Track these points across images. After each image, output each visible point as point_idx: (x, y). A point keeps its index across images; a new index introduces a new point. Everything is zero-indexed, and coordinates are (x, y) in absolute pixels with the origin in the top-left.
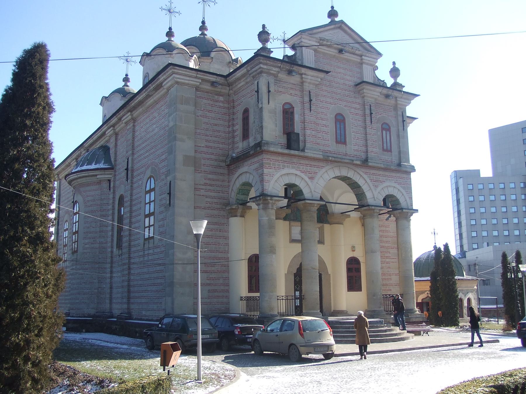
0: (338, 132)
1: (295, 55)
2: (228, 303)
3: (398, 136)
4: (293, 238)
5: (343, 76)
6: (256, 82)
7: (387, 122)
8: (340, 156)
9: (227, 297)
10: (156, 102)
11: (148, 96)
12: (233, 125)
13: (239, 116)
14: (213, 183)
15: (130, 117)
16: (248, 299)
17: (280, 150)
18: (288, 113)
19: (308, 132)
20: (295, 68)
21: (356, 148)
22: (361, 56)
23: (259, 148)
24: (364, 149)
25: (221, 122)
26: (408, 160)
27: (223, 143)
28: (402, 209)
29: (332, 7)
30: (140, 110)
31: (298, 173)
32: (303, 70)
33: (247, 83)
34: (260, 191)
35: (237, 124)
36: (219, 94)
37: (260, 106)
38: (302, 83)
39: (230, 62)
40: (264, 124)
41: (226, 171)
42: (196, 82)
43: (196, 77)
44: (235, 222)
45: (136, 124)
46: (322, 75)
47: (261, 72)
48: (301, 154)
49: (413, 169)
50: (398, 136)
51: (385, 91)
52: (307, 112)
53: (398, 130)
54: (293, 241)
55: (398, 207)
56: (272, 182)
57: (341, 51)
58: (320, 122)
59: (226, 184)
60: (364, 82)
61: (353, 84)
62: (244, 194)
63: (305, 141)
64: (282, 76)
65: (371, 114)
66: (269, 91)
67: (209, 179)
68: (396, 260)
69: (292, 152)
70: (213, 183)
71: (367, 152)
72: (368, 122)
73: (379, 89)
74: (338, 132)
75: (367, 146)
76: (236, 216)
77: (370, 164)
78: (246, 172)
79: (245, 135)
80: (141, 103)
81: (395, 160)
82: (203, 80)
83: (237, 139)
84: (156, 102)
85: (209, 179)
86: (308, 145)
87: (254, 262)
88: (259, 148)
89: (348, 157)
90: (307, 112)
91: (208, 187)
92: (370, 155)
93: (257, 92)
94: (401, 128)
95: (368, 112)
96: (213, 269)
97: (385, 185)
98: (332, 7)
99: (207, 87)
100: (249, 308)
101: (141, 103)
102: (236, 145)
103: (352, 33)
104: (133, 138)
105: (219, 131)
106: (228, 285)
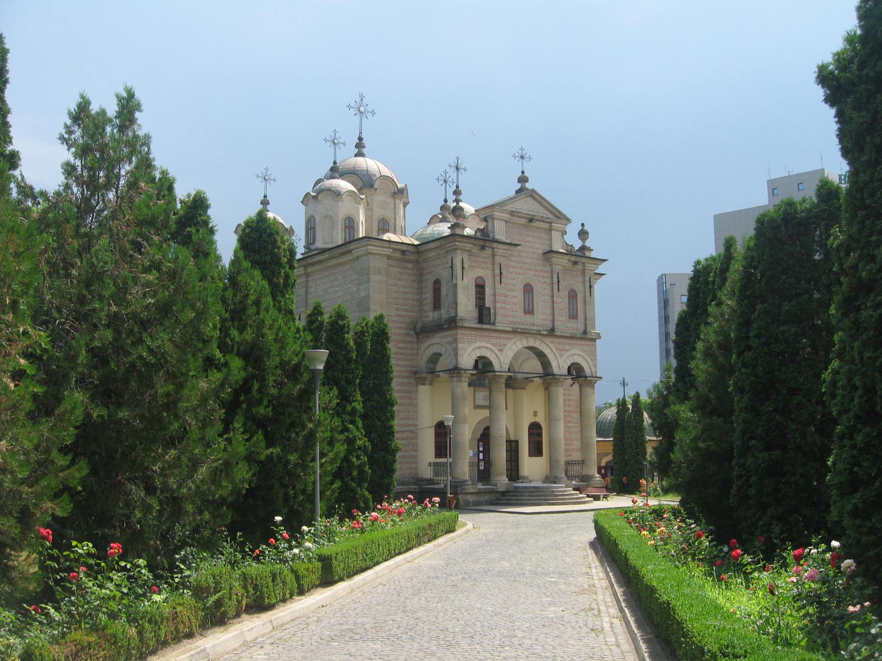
0: (527, 302)
1: (486, 227)
2: (416, 469)
3: (585, 302)
4: (477, 404)
5: (533, 244)
6: (450, 257)
7: (575, 288)
8: (527, 327)
9: (416, 463)
10: (341, 265)
11: (332, 258)
12: (421, 293)
13: (430, 286)
14: (403, 351)
15: (303, 272)
16: (435, 465)
17: (473, 326)
18: (480, 288)
19: (498, 305)
20: (488, 244)
21: (543, 317)
22: (550, 223)
23: (452, 323)
24: (550, 318)
25: (410, 290)
26: (594, 328)
27: (412, 311)
28: (586, 377)
29: (523, 172)
30: (318, 267)
31: (489, 346)
32: (495, 245)
33: (439, 254)
34: (454, 363)
35: (427, 292)
36: (408, 261)
37: (455, 282)
38: (493, 256)
39: (395, 193)
40: (459, 300)
41: (415, 340)
42: (388, 252)
43: (388, 248)
44: (424, 391)
45: (309, 279)
46: (512, 248)
47: (456, 249)
48: (492, 327)
49: (599, 336)
50: (585, 302)
51: (573, 259)
52: (497, 284)
53: (585, 297)
54: (477, 407)
55: (582, 374)
56: (465, 356)
57: (531, 220)
58: (509, 293)
59: (415, 352)
60: (551, 251)
61: (541, 252)
62: (432, 363)
63: (495, 314)
64: (476, 250)
65: (559, 282)
66: (463, 268)
67: (400, 348)
68: (579, 425)
69: (485, 326)
70: (403, 351)
71: (553, 321)
72: (556, 291)
73: (568, 257)
74: (527, 302)
75: (553, 315)
76: (424, 384)
77: (557, 334)
78: (436, 343)
79: (437, 305)
80: (320, 262)
81: (582, 329)
82: (394, 249)
83: (427, 308)
84: (341, 265)
85: (400, 348)
86: (498, 318)
87: (441, 430)
88: (452, 323)
89: (535, 328)
90: (497, 284)
91: (399, 356)
92: (557, 324)
93: (452, 267)
94: (588, 294)
95: (555, 280)
96: (403, 435)
97: (570, 353)
98: (523, 172)
99: (398, 255)
100: (436, 474)
101: (320, 262)
102: (425, 314)
103: (543, 201)
104: (307, 293)
105: (408, 299)
106: (416, 451)
